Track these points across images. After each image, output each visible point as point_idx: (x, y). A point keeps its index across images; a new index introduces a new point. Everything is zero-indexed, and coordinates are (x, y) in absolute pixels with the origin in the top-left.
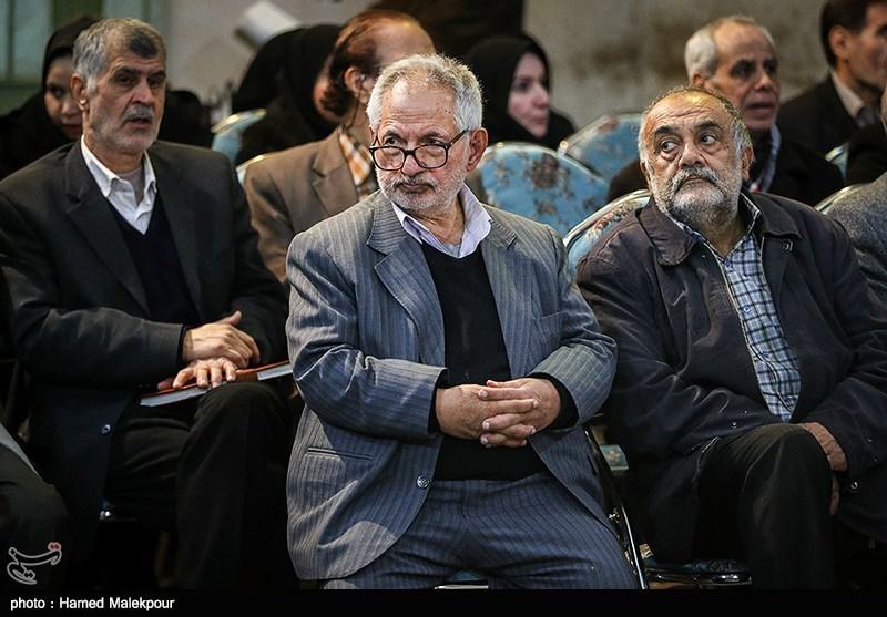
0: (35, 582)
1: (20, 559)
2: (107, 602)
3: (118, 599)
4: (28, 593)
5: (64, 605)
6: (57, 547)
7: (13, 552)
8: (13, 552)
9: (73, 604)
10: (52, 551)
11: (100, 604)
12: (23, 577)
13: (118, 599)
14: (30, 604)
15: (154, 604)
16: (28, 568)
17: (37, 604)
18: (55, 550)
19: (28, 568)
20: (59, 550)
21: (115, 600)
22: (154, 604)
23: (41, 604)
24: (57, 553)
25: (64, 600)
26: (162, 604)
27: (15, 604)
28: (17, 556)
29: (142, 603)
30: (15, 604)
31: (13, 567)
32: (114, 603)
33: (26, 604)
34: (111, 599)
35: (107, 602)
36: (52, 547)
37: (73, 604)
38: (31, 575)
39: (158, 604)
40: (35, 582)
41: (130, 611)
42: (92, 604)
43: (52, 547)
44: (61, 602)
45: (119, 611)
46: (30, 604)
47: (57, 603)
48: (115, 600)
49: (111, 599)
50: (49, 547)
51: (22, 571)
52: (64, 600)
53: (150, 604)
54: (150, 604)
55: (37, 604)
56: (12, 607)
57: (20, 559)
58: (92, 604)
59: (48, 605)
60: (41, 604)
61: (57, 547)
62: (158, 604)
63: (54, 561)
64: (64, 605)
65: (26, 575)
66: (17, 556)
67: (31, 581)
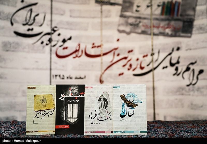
2: (25, 141)
3: (28, 140)
4: (7, 139)
5: (15, 141)
9: (17, 141)
10: (12, 128)
11: (23, 141)
13: (28, 140)
14: (7, 141)
15: (36, 141)
16: (7, 133)
19: (7, 133)
21: (27, 140)
22: (36, 141)
23: (10, 141)
24: (13, 129)
25: (15, 140)
26: (38, 141)
27: (4, 141)
28: (4, 130)
29: (33, 141)
30: (4, 141)
31: (3, 132)
32: (27, 141)
33: (6, 141)
34: (26, 140)
35: (25, 141)
37: (17, 141)
39: (37, 141)
41: (30, 143)
42: (21, 141)
44: (14, 141)
45: (28, 143)
46: (7, 141)
47: (13, 141)
48: (27, 140)
49: (26, 140)
51: (5, 133)
52: (15, 140)
53: (35, 141)
54: (35, 141)
56: (3, 142)
58: (21, 141)
59: (11, 141)
60: (10, 141)
62: (37, 141)
63: (12, 131)
64: (15, 141)
65: (6, 134)
66: (4, 130)
67: (8, 136)
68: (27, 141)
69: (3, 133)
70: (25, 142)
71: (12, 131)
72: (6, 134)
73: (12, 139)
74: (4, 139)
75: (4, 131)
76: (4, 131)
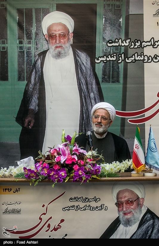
0: (10, 237)
7: (4, 228)
8: (4, 228)
10: (15, 228)
14: (9, 242)
18: (15, 228)
23: (12, 242)
24: (16, 229)
30: (5, 243)
31: (4, 233)
36: (15, 227)
38: (9, 235)
40: (10, 237)
43: (15, 227)
46: (9, 242)
50: (14, 227)
51: (6, 234)
56: (4, 243)
59: (14, 243)
60: (12, 242)
61: (16, 227)
65: (8, 235)
69: (5, 234)
72: (8, 235)
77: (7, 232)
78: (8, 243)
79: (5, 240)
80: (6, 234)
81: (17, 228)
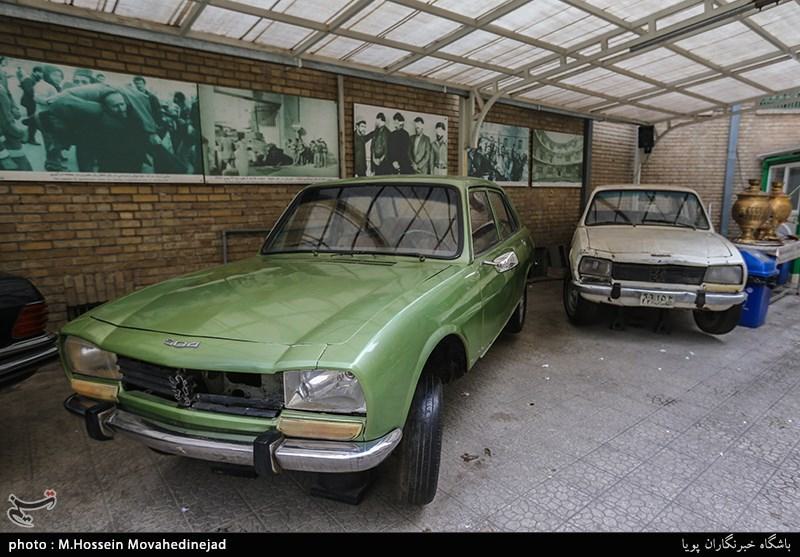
0: (33, 526)
1: (19, 504)
3: (136, 541)
5: (78, 546)
6: (52, 493)
7: (12, 498)
8: (12, 498)
12: (23, 522)
13: (136, 541)
16: (27, 513)
17: (43, 546)
18: (50, 496)
19: (27, 513)
20: (54, 497)
21: (133, 542)
23: (43, 546)
24: (52, 500)
28: (16, 502)
31: (12, 512)
36: (48, 494)
38: (29, 519)
40: (33, 526)
44: (76, 544)
48: (133, 542)
50: (45, 494)
51: (21, 515)
55: (43, 546)
56: (11, 548)
57: (19, 504)
60: (43, 546)
61: (52, 493)
64: (78, 546)
66: (16, 502)
67: (28, 526)
68: (133, 545)
70: (126, 551)
71: (49, 506)
73: (52, 538)
74: (14, 537)
75: (17, 508)
76: (21, 510)
77: (21, 510)
78: (29, 546)
79: (14, 537)
80: (21, 515)
81: (54, 497)
